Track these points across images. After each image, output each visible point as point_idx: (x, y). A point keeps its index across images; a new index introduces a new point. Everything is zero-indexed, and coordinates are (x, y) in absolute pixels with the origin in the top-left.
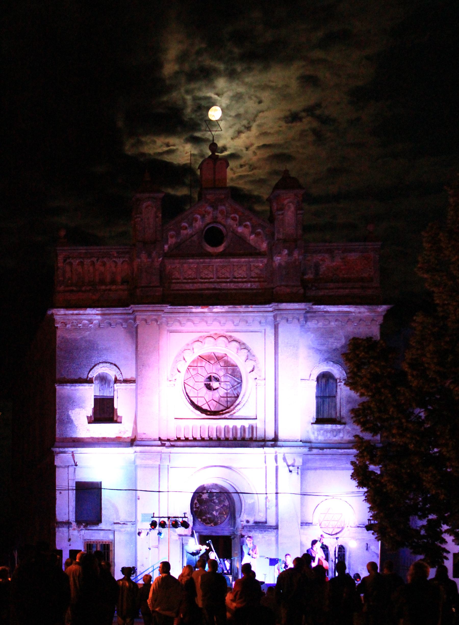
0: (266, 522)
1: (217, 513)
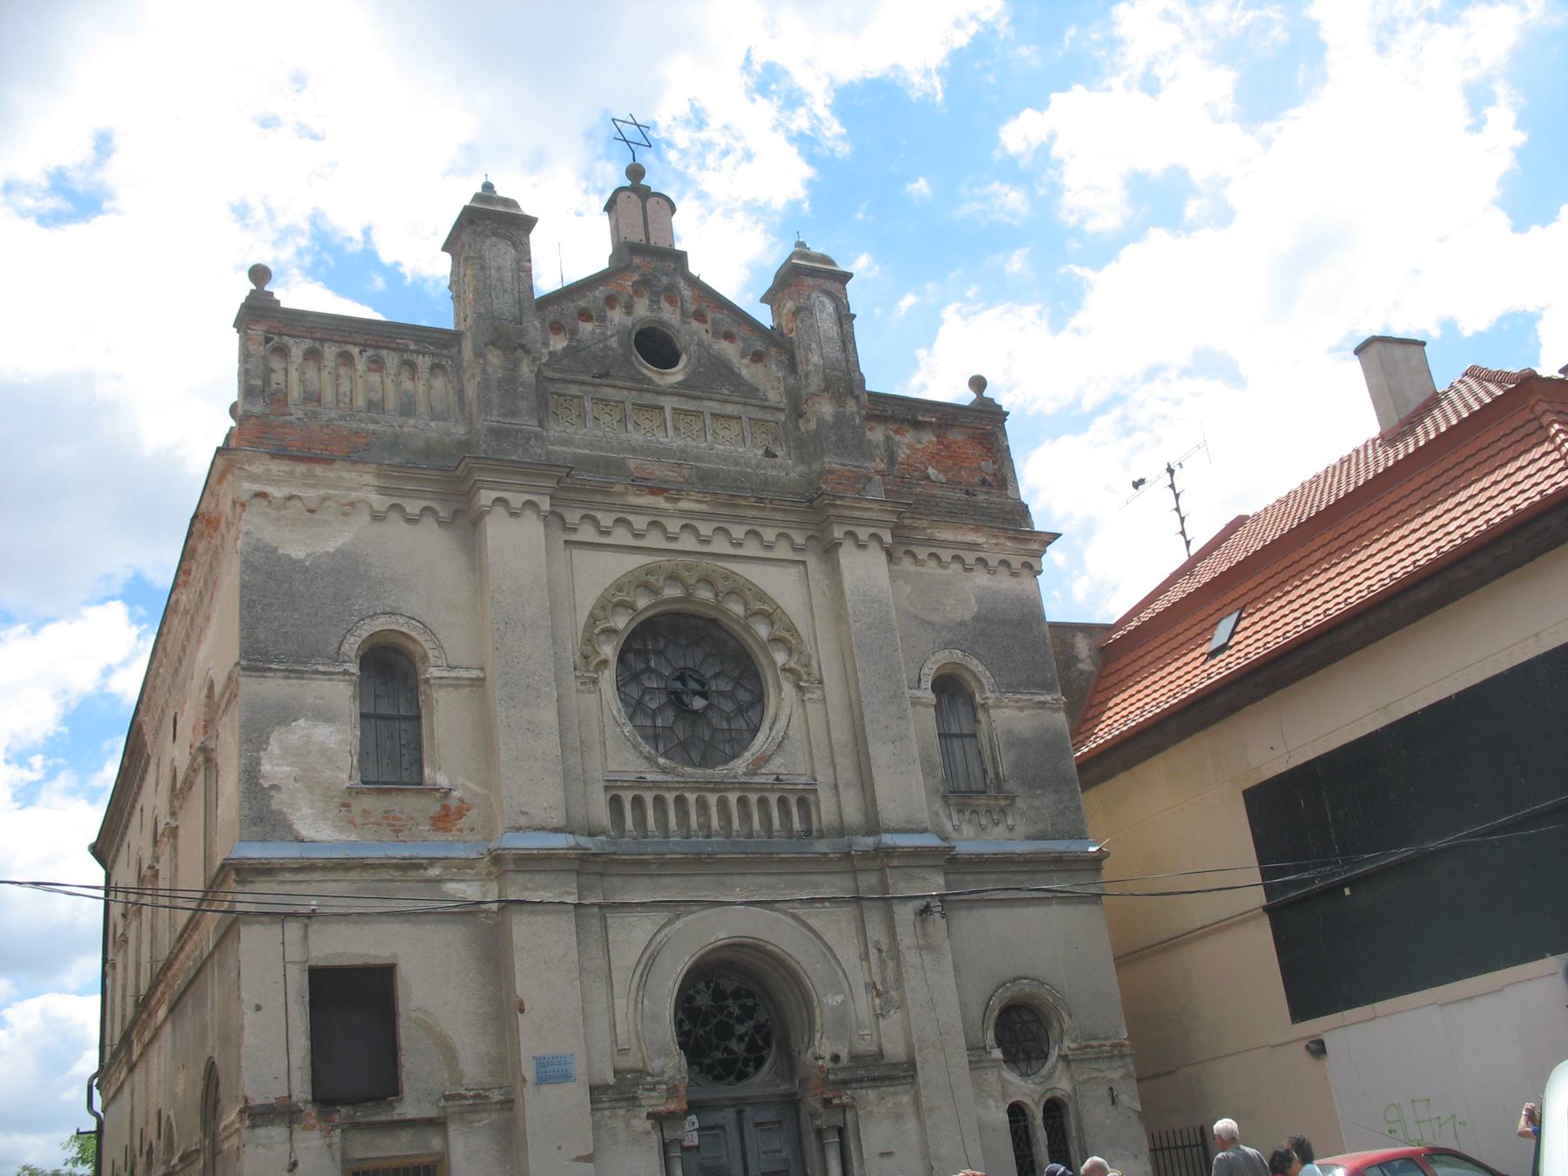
0: (880, 1054)
1: (743, 1046)
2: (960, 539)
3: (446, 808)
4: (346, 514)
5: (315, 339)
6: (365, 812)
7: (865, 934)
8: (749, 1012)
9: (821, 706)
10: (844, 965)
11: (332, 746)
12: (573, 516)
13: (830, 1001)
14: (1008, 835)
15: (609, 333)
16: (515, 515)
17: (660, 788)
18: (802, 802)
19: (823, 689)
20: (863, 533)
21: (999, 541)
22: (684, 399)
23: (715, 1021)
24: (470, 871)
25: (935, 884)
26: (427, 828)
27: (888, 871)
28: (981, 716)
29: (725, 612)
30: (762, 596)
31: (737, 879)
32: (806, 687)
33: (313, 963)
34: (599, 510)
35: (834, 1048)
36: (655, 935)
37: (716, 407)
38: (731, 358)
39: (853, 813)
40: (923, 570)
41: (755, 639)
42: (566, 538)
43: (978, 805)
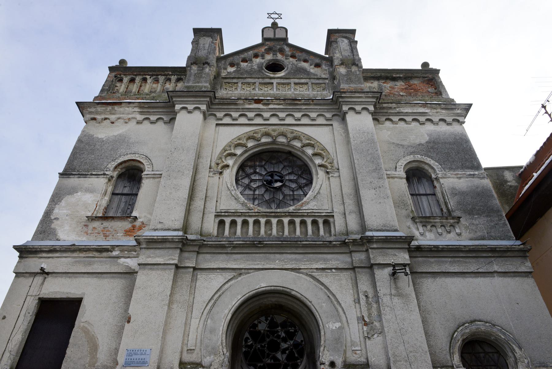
1: (285, 356)
2: (415, 111)
3: (134, 227)
4: (126, 123)
5: (133, 75)
6: (94, 228)
7: (357, 287)
8: (290, 336)
9: (338, 179)
10: (343, 305)
11: (89, 202)
12: (220, 115)
13: (331, 326)
14: (457, 237)
15: (254, 65)
16: (190, 112)
17: (245, 216)
18: (326, 223)
19: (339, 172)
20: (358, 108)
21: (437, 111)
22: (282, 79)
23: (268, 340)
24: (134, 253)
25: (403, 257)
26: (122, 234)
27: (370, 250)
28: (436, 183)
29: (293, 147)
30: (309, 138)
31: (278, 256)
32: (330, 172)
33: (41, 296)
34: (233, 111)
35: (332, 358)
36: (225, 284)
37: (297, 81)
38: (306, 67)
39: (353, 224)
40: (397, 126)
41: (306, 155)
42: (217, 123)
43: (435, 222)
